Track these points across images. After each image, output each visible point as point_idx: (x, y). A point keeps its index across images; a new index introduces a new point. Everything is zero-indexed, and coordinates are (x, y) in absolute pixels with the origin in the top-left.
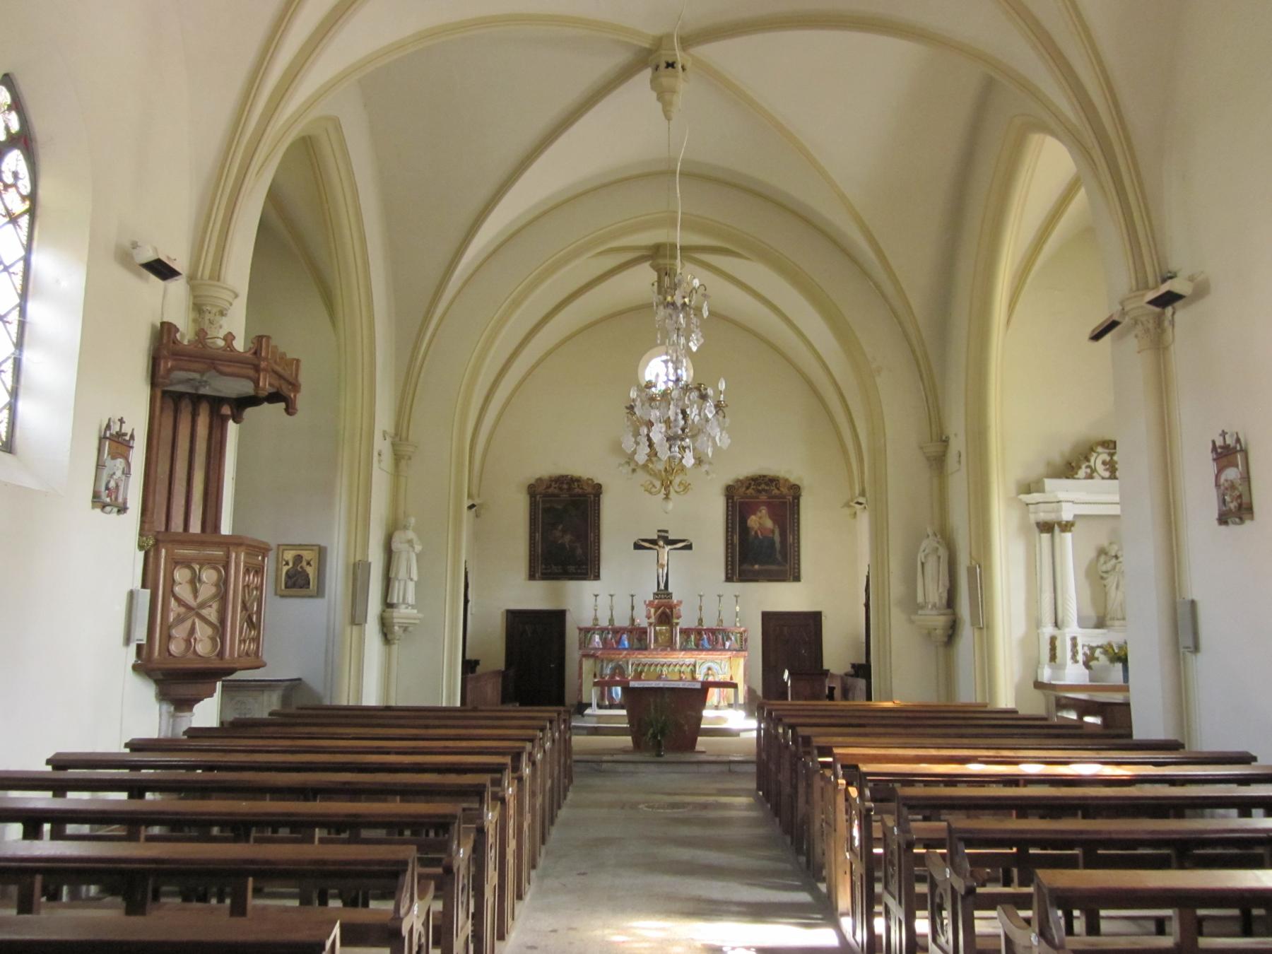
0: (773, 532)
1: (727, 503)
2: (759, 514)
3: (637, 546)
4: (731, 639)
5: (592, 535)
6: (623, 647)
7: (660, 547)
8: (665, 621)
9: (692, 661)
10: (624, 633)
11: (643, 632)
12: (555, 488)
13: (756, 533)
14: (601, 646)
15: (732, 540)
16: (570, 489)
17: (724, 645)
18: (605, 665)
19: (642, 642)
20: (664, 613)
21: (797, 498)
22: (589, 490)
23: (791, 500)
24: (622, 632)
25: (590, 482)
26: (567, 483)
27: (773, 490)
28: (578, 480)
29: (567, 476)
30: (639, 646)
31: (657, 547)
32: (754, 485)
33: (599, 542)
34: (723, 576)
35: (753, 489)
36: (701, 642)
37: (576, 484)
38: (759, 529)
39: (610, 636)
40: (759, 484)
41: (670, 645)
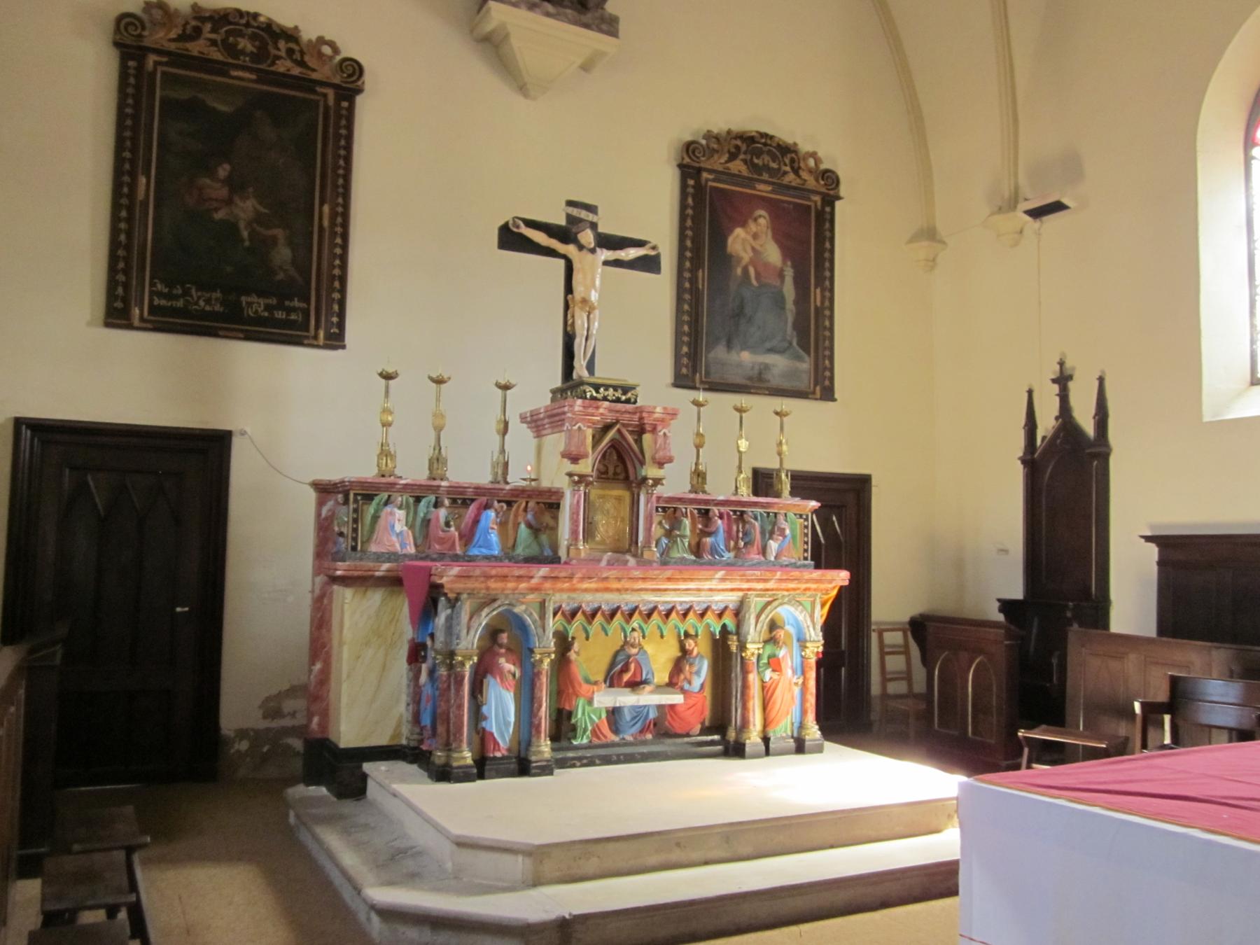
0: (781, 276)
1: (684, 186)
2: (753, 227)
3: (511, 239)
4: (782, 531)
5: (326, 209)
6: (485, 551)
7: (581, 247)
8: (615, 474)
9: (732, 598)
10: (487, 506)
11: (550, 502)
12: (213, 43)
13: (745, 270)
14: (411, 550)
15: (693, 281)
16: (261, 55)
17: (764, 551)
18: (465, 617)
19: (544, 538)
20: (615, 446)
21: (830, 200)
22: (322, 73)
23: (819, 204)
24: (484, 499)
25: (327, 50)
26: (253, 37)
27: (785, 173)
28: (291, 36)
29: (255, 16)
30: (534, 550)
31: (570, 250)
32: (745, 153)
33: (345, 237)
34: (668, 374)
35: (745, 161)
36: (708, 540)
37: (282, 44)
38: (752, 262)
39: (442, 513)
40: (758, 154)
41: (628, 546)
